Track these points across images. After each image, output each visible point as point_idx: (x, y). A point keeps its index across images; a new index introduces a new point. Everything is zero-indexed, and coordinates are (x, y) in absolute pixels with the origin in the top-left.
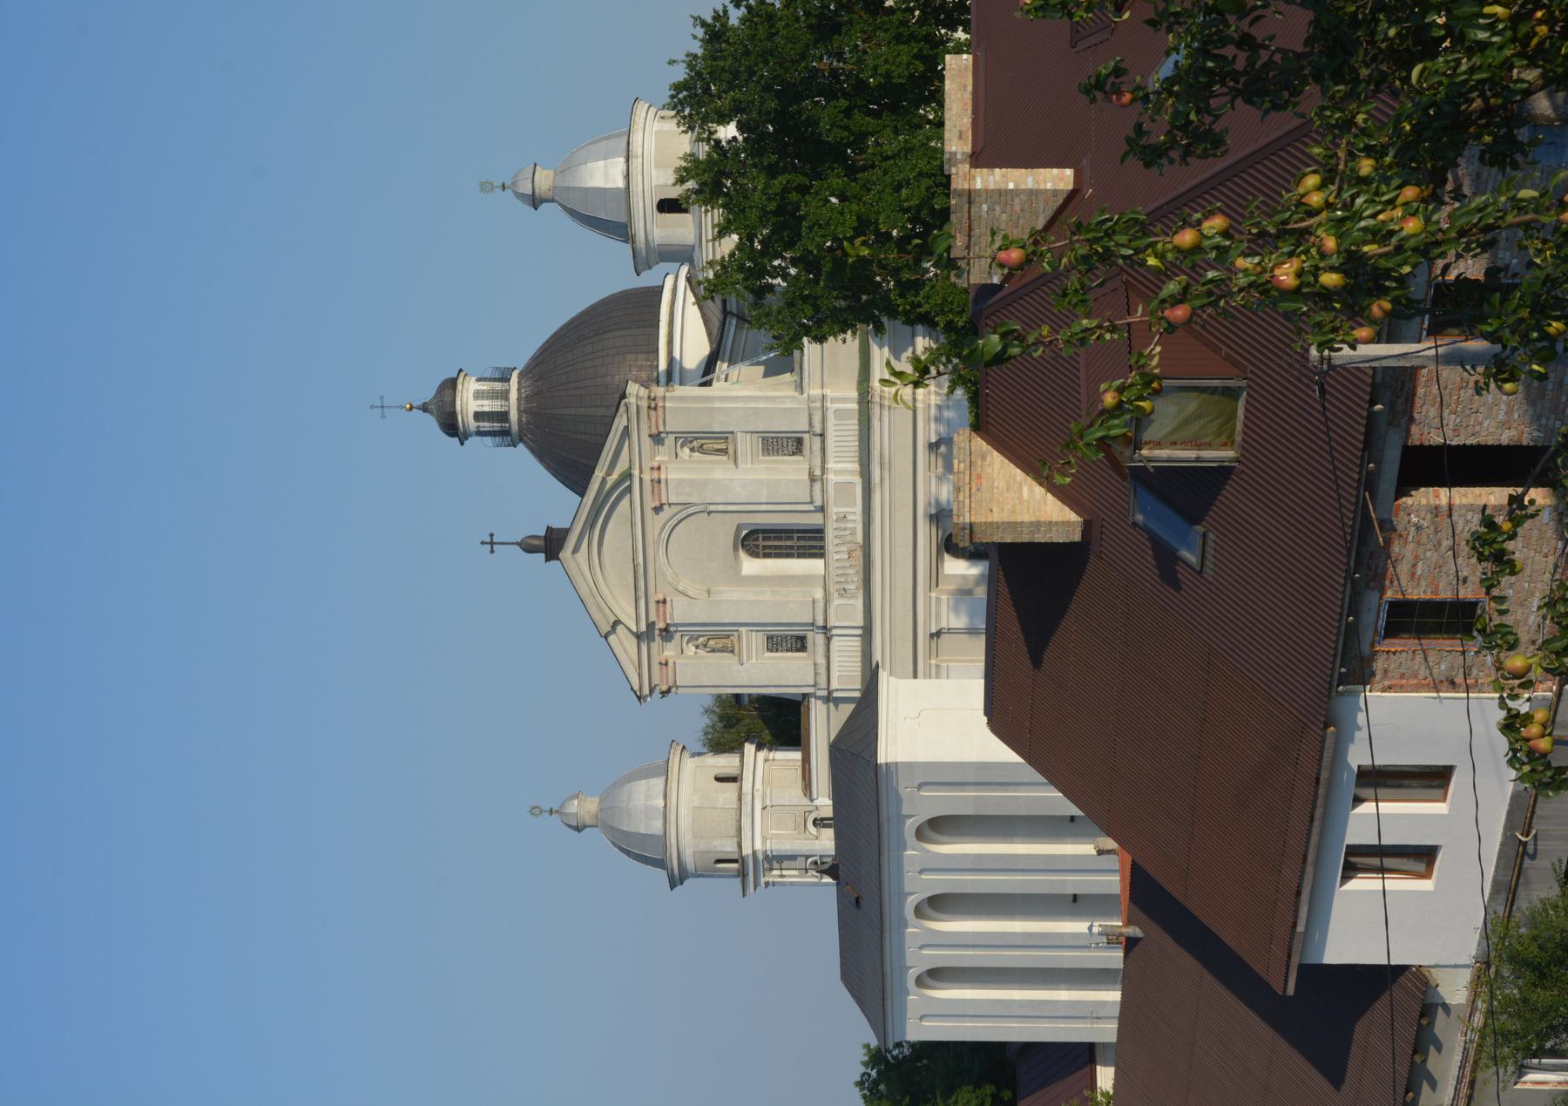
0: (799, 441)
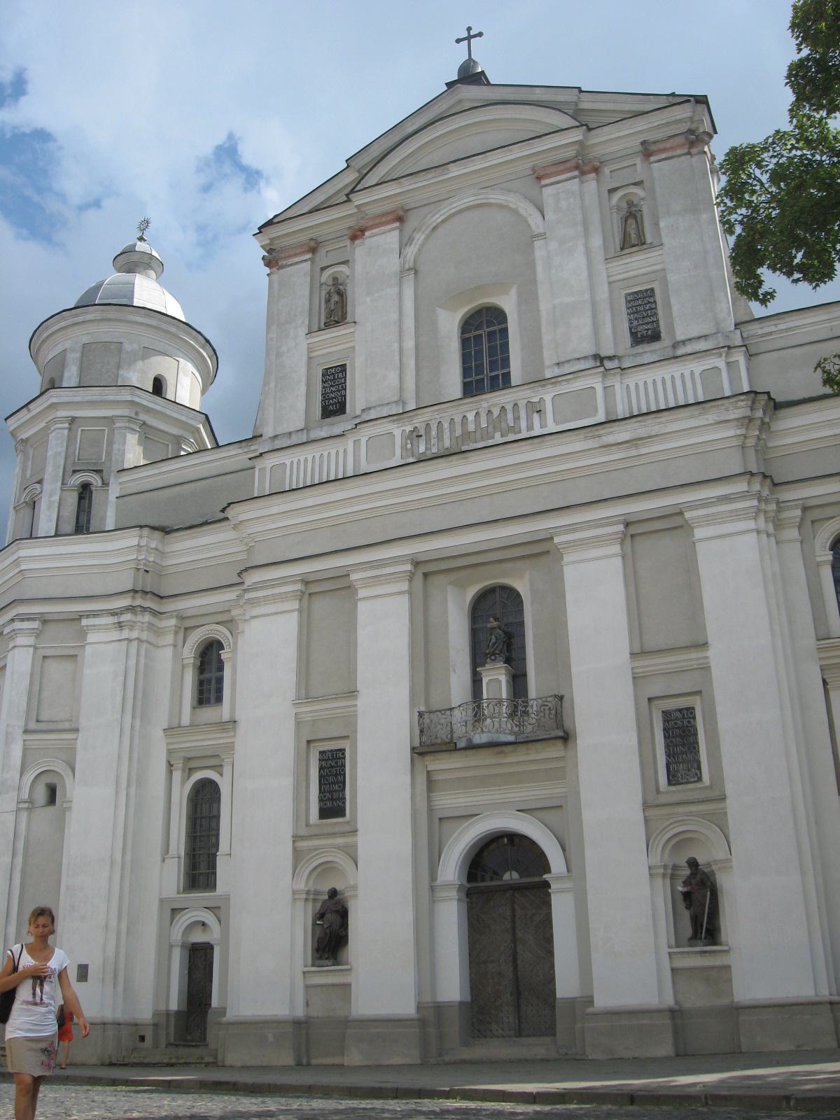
0: (655, 337)
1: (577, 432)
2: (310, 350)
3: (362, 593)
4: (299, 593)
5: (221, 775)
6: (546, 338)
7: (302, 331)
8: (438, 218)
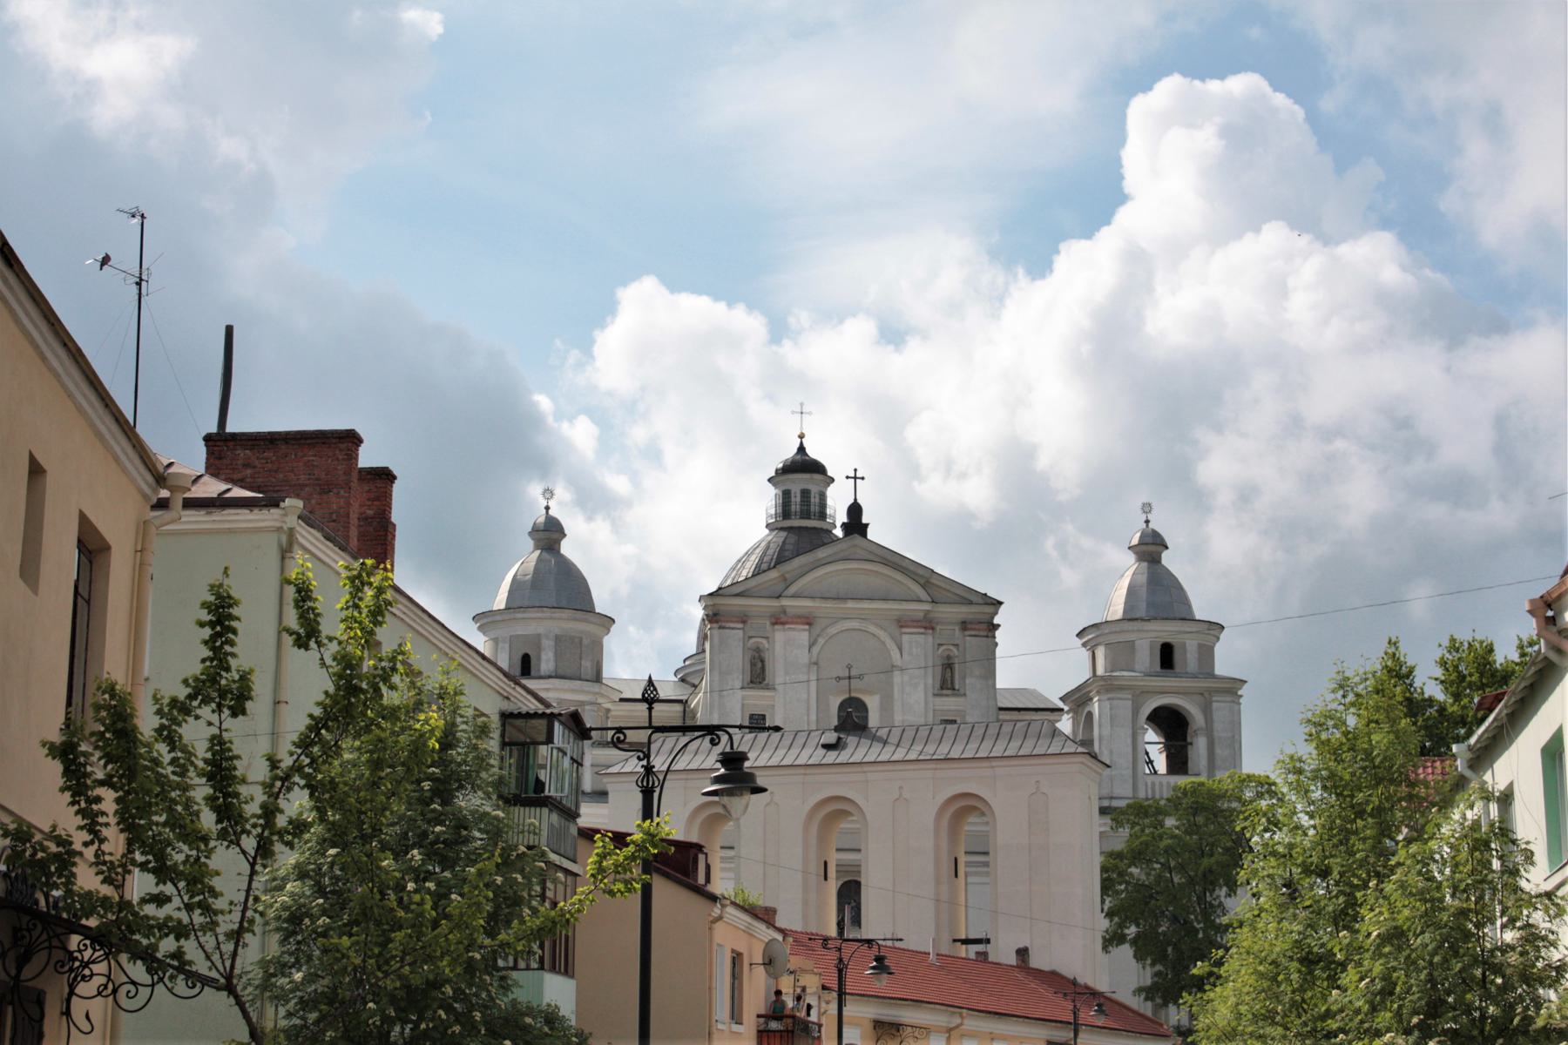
2: (743, 698)
7: (738, 684)
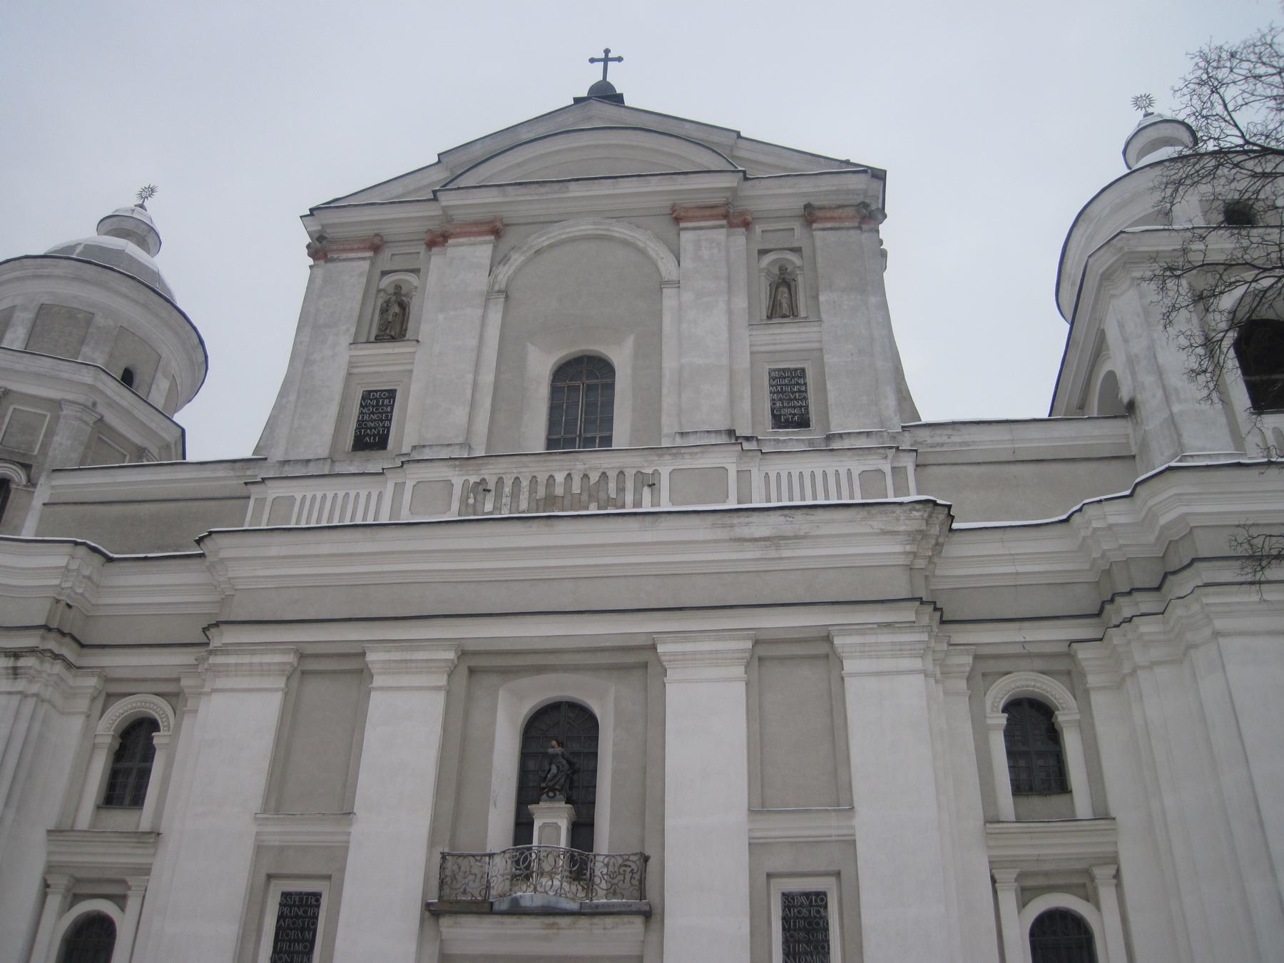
0: (804, 423)
1: (702, 516)
2: (352, 365)
3: (378, 681)
4: (288, 667)
5: (123, 909)
6: (668, 400)
7: (346, 340)
8: (544, 241)
